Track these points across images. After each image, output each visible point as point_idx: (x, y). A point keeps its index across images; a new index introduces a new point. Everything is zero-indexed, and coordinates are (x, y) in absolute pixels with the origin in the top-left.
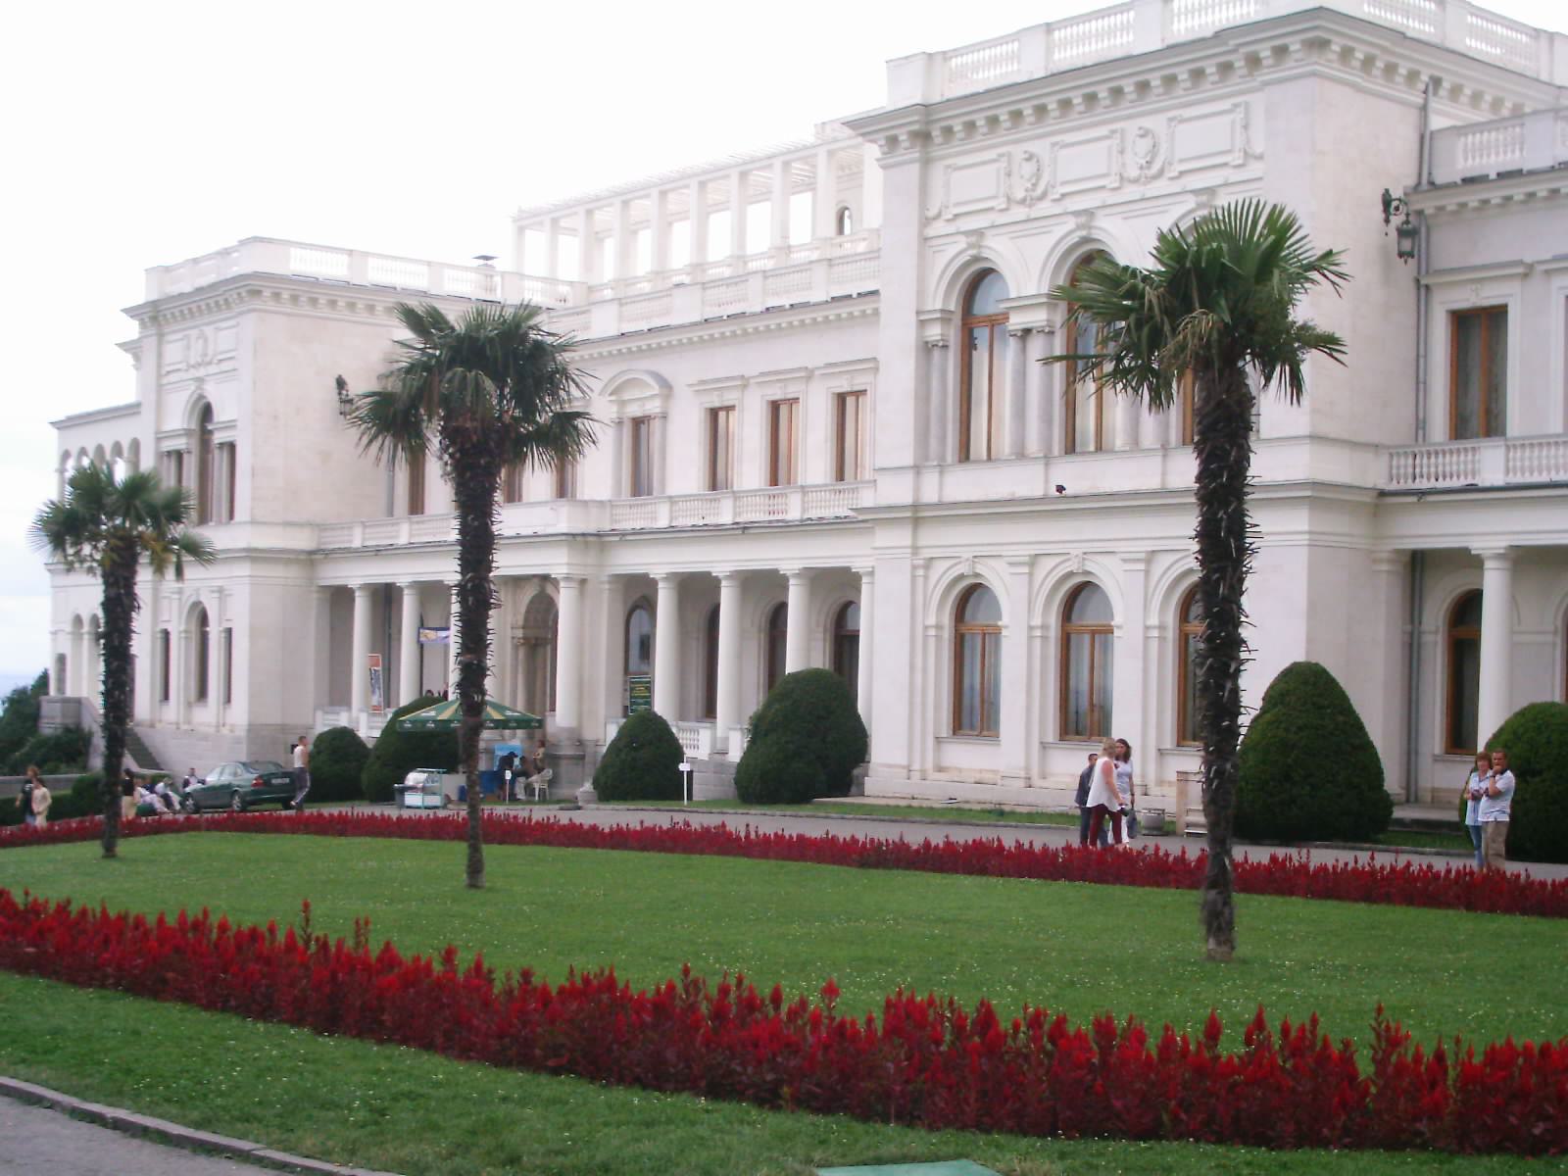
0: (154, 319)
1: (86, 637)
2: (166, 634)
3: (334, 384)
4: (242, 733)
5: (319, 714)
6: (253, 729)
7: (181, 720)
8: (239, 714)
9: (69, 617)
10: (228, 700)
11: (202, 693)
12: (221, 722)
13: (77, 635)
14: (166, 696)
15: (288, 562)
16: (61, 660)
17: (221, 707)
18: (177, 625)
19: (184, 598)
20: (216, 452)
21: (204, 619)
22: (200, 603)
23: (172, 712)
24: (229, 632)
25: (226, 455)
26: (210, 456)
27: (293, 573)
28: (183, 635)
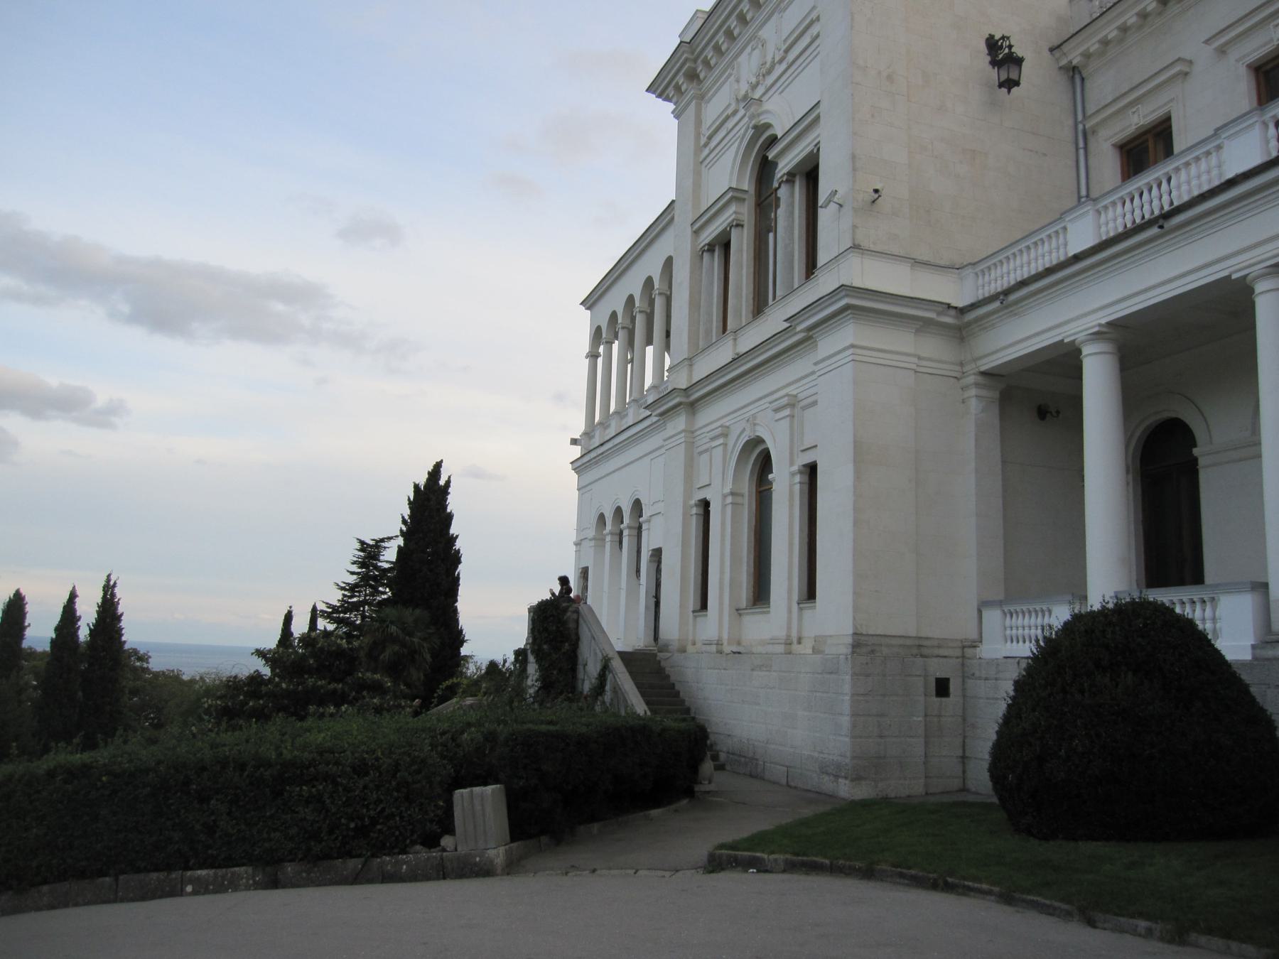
0: (693, 76)
1: (608, 538)
2: (705, 504)
3: (983, 47)
4: (841, 648)
5: (993, 617)
6: (860, 643)
7: (725, 636)
8: (834, 616)
9: (593, 519)
10: (810, 593)
11: (761, 593)
12: (794, 634)
13: (599, 540)
14: (704, 605)
15: (924, 326)
16: (584, 573)
17: (795, 607)
18: (722, 481)
19: (731, 442)
20: (783, 193)
21: (765, 463)
22: (759, 441)
23: (713, 625)
24: (812, 470)
25: (798, 189)
26: (771, 235)
27: (933, 348)
28: (729, 499)
